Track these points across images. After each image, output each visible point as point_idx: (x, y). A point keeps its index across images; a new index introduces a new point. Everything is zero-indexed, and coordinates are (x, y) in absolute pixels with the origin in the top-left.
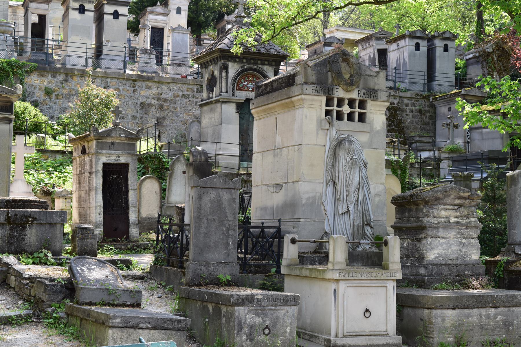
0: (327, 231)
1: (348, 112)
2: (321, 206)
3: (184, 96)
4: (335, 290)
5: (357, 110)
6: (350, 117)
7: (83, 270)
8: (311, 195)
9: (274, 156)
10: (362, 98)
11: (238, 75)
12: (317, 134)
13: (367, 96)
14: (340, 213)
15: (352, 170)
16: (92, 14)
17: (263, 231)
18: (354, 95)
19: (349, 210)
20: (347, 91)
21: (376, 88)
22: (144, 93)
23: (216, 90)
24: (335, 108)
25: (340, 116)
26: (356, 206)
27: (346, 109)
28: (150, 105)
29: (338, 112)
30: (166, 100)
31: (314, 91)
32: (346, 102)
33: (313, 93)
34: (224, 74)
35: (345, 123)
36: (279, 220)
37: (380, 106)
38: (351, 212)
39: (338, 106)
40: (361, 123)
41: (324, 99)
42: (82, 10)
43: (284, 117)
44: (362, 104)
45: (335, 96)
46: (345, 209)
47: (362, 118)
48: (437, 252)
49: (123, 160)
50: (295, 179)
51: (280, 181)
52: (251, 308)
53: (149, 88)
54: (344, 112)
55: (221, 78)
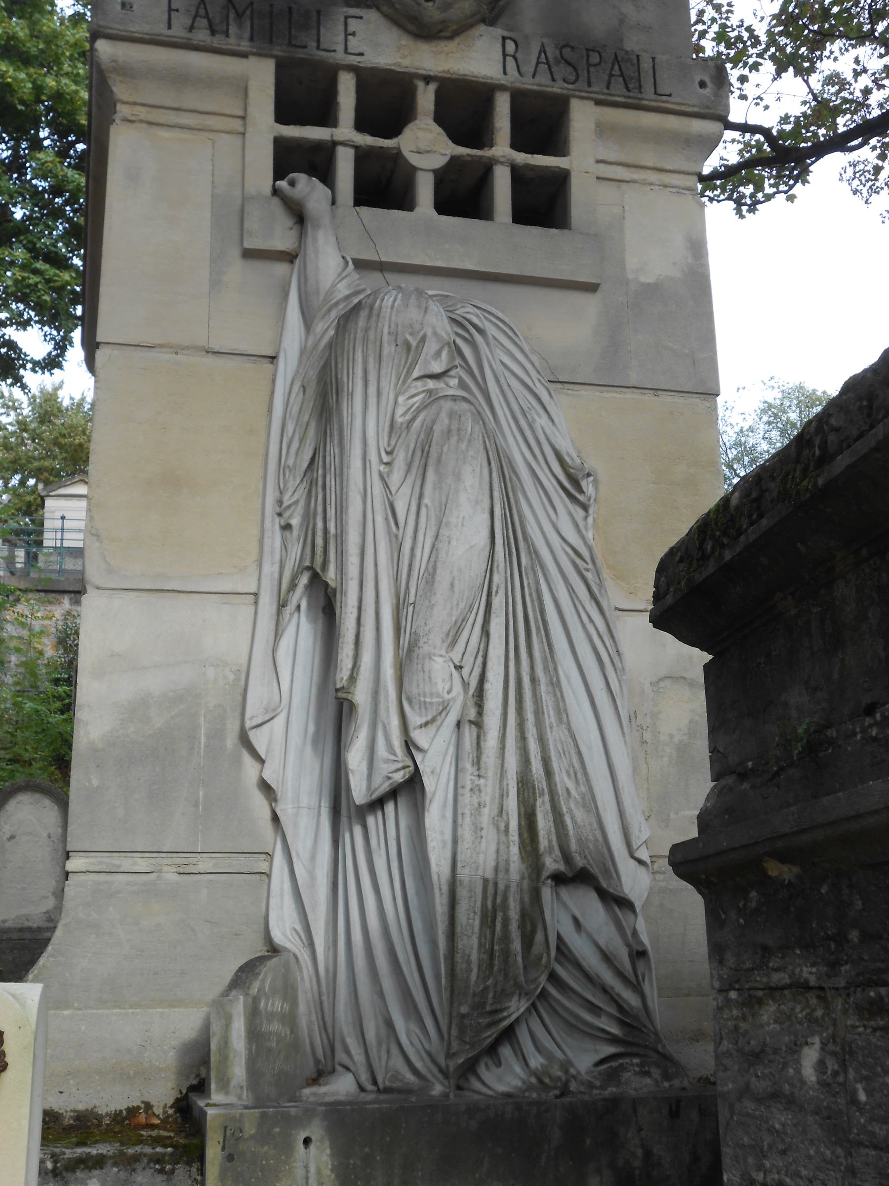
0: (278, 936)
1: (439, 162)
2: (237, 762)
5: (502, 148)
6: (463, 195)
8: (155, 683)
10: (528, 84)
12: (216, 283)
13: (562, 70)
15: (431, 476)
21: (633, 43)
24: (345, 129)
26: (469, 733)
27: (425, 146)
33: (178, 31)
37: (659, 138)
39: (360, 125)
40: (535, 231)
41: (261, 76)
44: (541, 126)
45: (340, 57)
47: (543, 203)
54: (414, 160)
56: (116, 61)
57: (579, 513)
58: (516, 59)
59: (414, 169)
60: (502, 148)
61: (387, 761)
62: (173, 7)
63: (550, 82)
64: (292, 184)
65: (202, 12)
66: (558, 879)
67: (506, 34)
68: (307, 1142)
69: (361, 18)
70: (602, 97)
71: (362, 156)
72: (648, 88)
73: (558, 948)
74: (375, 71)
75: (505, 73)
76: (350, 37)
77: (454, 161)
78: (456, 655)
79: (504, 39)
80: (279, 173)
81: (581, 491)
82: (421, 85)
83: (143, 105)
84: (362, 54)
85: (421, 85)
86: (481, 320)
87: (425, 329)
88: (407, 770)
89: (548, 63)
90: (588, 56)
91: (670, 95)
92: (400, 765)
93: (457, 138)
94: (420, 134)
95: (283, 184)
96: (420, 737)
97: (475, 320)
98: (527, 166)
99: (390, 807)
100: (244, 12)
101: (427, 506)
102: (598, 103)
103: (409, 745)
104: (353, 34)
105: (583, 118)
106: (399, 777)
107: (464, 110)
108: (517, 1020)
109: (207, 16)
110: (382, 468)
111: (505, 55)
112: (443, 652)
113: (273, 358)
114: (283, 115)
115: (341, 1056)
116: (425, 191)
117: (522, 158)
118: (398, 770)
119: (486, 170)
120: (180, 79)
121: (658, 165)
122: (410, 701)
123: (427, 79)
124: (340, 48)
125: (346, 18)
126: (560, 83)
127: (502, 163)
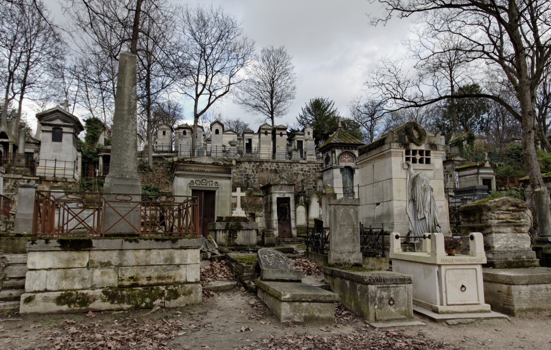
3: (313, 169)
4: (438, 272)
5: (425, 156)
6: (421, 161)
7: (265, 257)
8: (399, 208)
9: (373, 187)
11: (341, 155)
14: (419, 218)
16: (271, 135)
17: (371, 230)
18: (423, 147)
19: (425, 217)
20: (418, 145)
21: (435, 143)
22: (296, 168)
23: (330, 163)
24: (411, 156)
25: (414, 161)
27: (418, 157)
28: (298, 174)
29: (413, 158)
30: (305, 171)
32: (418, 152)
34: (334, 155)
35: (418, 165)
36: (383, 224)
37: (438, 154)
41: (404, 151)
42: (266, 133)
43: (379, 164)
44: (428, 153)
46: (422, 216)
47: (428, 161)
48: (500, 243)
49: (287, 196)
50: (389, 199)
51: (377, 202)
52: (379, 286)
53: (297, 166)
55: (332, 157)
60: (425, 156)
105: (432, 152)
114: (406, 155)
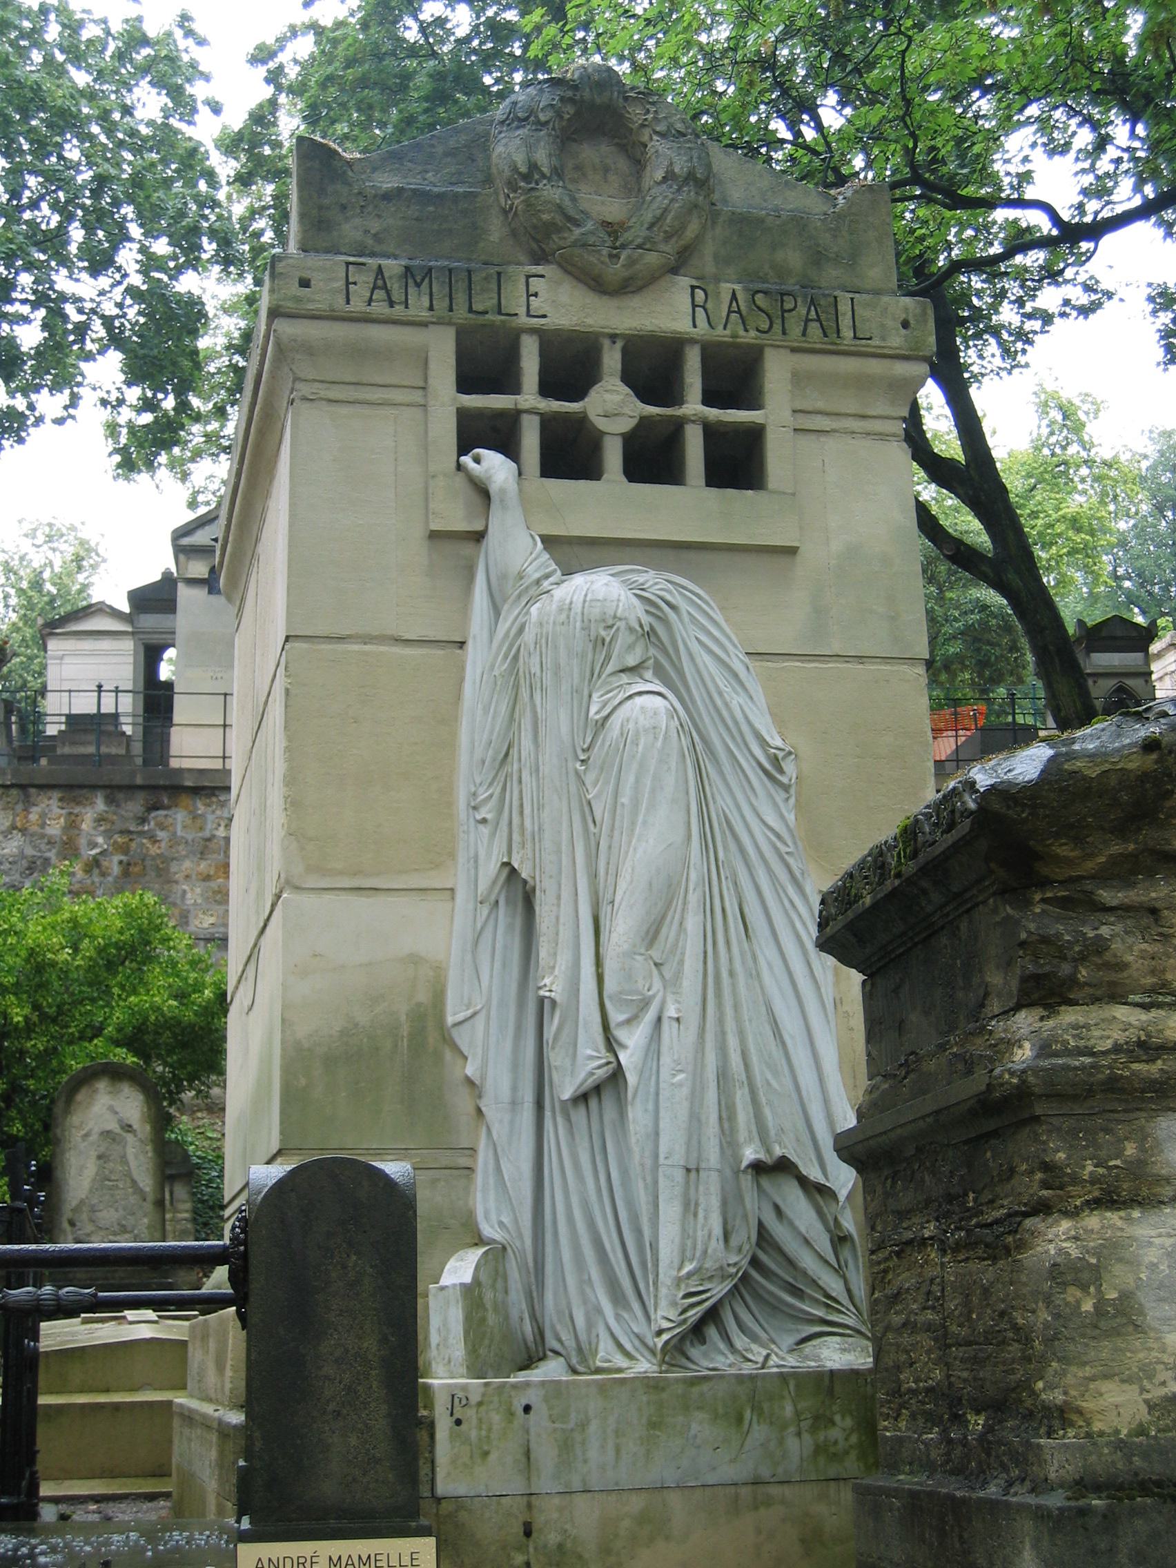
1: (626, 425)
5: (693, 406)
6: (652, 459)
10: (721, 334)
18: (670, 312)
24: (529, 397)
25: (569, 455)
27: (612, 406)
31: (360, 292)
32: (612, 360)
33: (357, 305)
38: (631, 1078)
39: (546, 390)
44: (734, 379)
45: (523, 320)
47: (737, 463)
54: (601, 424)
56: (295, 341)
57: (780, 796)
58: (706, 310)
59: (603, 434)
60: (693, 406)
61: (591, 1058)
62: (351, 280)
63: (742, 333)
64: (477, 460)
65: (380, 283)
66: (758, 1168)
67: (695, 283)
68: (527, 1409)
69: (542, 276)
70: (796, 344)
71: (548, 423)
72: (847, 333)
73: (760, 1233)
74: (558, 332)
75: (695, 326)
76: (532, 298)
77: (644, 422)
78: (656, 954)
79: (693, 288)
80: (464, 447)
81: (781, 771)
82: (606, 343)
83: (322, 382)
84: (544, 316)
85: (606, 343)
86: (674, 596)
87: (618, 624)
88: (611, 1066)
89: (739, 312)
90: (782, 301)
91: (870, 339)
92: (603, 1061)
93: (645, 395)
94: (607, 396)
95: (467, 460)
96: (620, 1034)
97: (668, 597)
98: (721, 423)
99: (593, 1103)
100: (423, 280)
101: (623, 805)
102: (794, 350)
103: (611, 1043)
104: (536, 295)
106: (602, 1073)
107: (653, 370)
108: (720, 1301)
109: (385, 287)
110: (578, 765)
111: (694, 306)
112: (642, 951)
113: (462, 644)
114: (465, 384)
115: (551, 1342)
116: (613, 457)
117: (713, 413)
118: (599, 1067)
119: (676, 428)
120: (359, 353)
121: (861, 412)
122: (610, 997)
123: (613, 337)
124: (522, 311)
125: (528, 277)
126: (753, 333)
127: (693, 422)
